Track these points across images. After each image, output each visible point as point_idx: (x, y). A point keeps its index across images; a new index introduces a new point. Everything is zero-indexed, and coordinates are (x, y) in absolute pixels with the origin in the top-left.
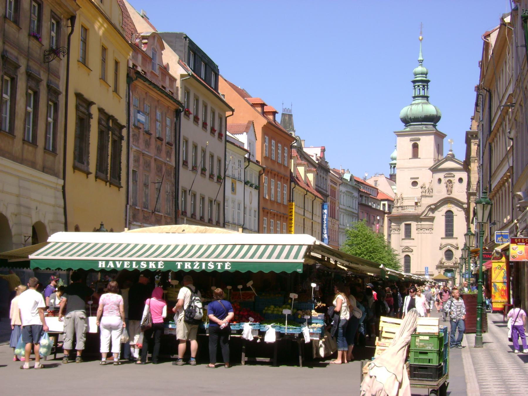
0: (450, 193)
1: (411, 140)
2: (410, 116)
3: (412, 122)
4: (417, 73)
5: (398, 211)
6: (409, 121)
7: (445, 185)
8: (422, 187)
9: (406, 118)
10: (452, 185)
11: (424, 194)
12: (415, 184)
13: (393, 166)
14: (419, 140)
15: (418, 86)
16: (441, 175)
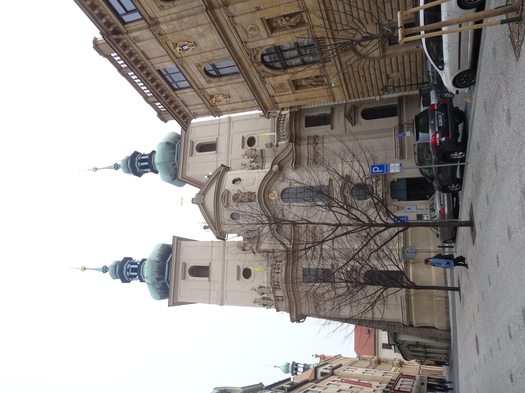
0: (252, 199)
1: (184, 278)
2: (154, 280)
3: (163, 278)
4: (114, 272)
5: (284, 299)
6: (161, 282)
7: (239, 204)
8: (244, 250)
9: (158, 287)
10: (241, 193)
11: (255, 247)
12: (247, 273)
13: (295, 372)
14: (185, 264)
15: (128, 270)
16: (225, 214)
